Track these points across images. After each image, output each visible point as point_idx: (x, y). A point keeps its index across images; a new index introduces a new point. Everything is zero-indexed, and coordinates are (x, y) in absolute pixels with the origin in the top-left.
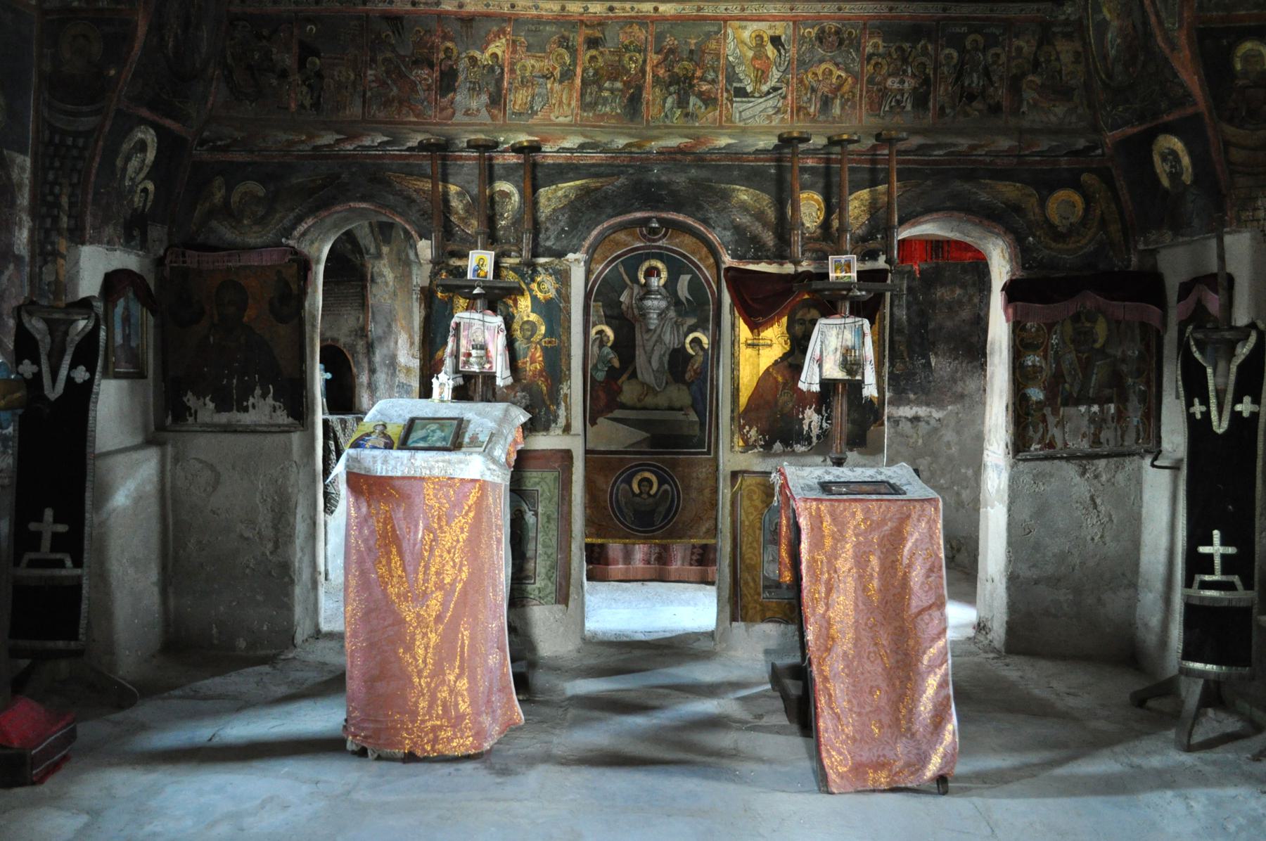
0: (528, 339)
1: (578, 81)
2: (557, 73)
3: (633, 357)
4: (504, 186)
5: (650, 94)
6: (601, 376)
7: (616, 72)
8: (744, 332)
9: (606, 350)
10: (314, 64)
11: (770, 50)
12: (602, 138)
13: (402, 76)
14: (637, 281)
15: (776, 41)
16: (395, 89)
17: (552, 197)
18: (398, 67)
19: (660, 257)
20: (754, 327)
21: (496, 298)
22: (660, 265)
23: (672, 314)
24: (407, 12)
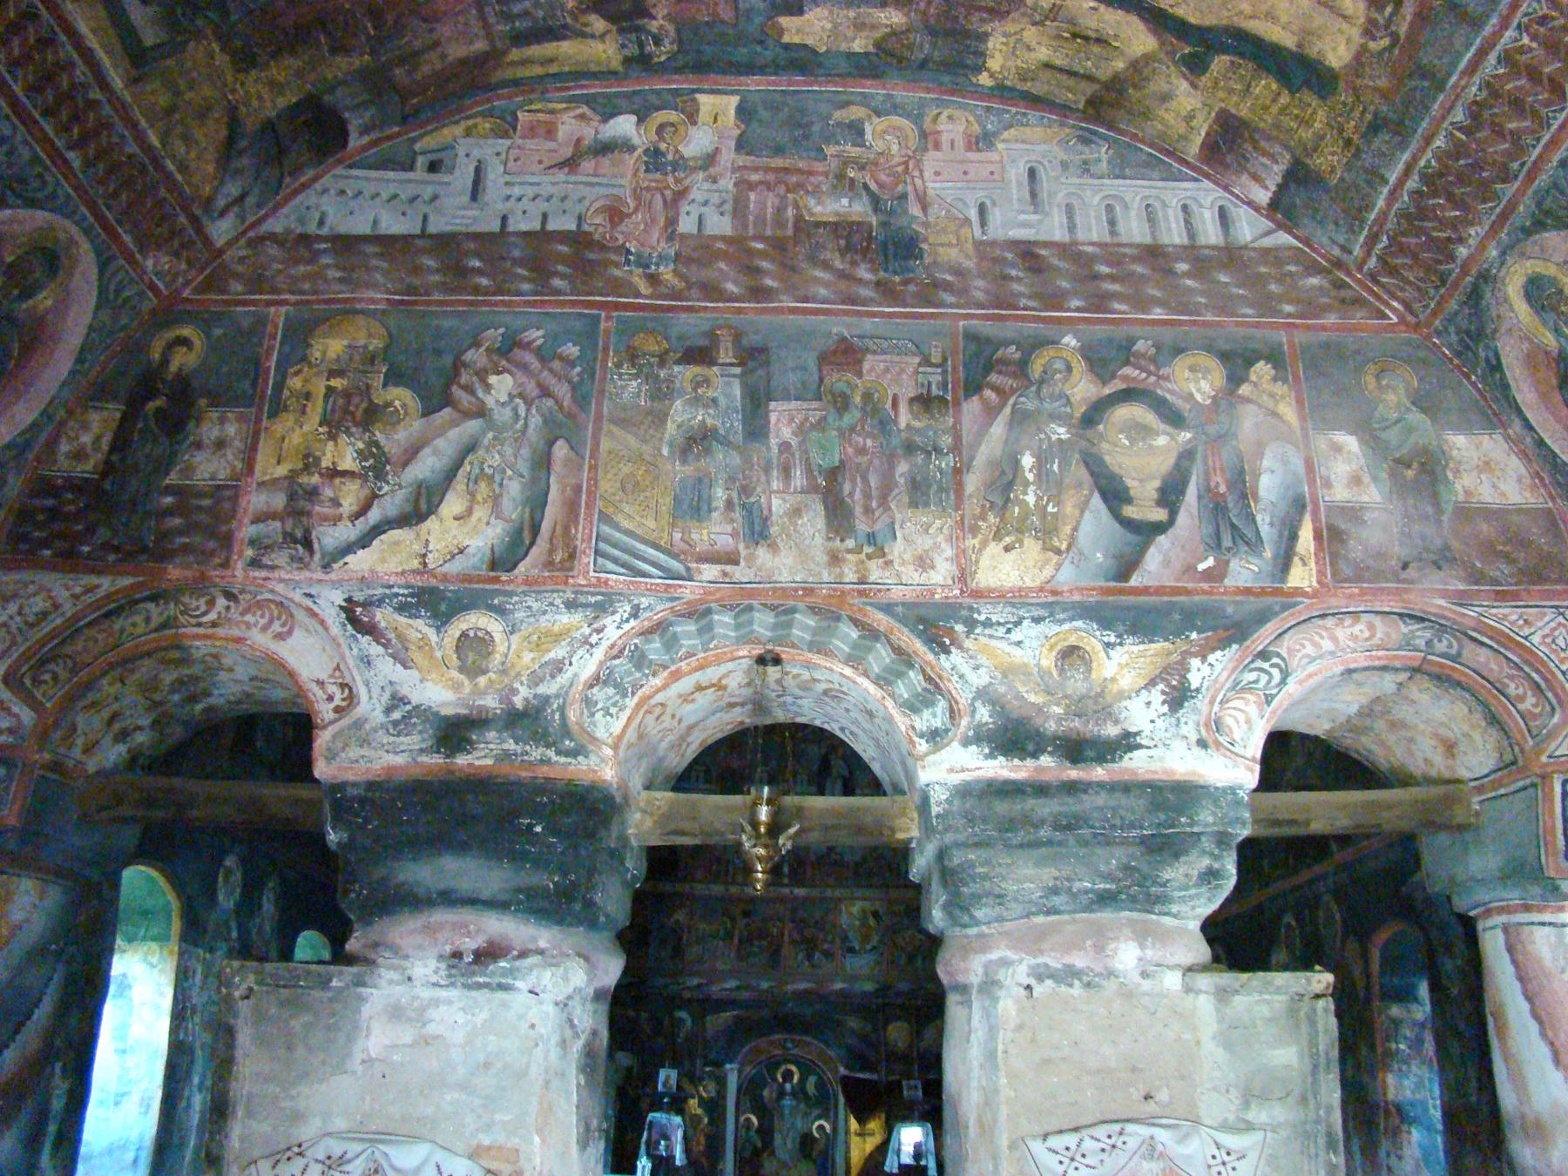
0: (695, 1129)
1: (736, 941)
2: (722, 933)
3: (772, 1138)
4: (683, 1014)
5: (786, 950)
6: (747, 1154)
7: (762, 934)
8: (854, 1124)
9: (752, 1133)
11: (872, 922)
12: (754, 983)
14: (775, 1079)
15: (875, 914)
17: (717, 1022)
19: (790, 1061)
20: (861, 1121)
21: (677, 1104)
22: (794, 1068)
23: (802, 1106)
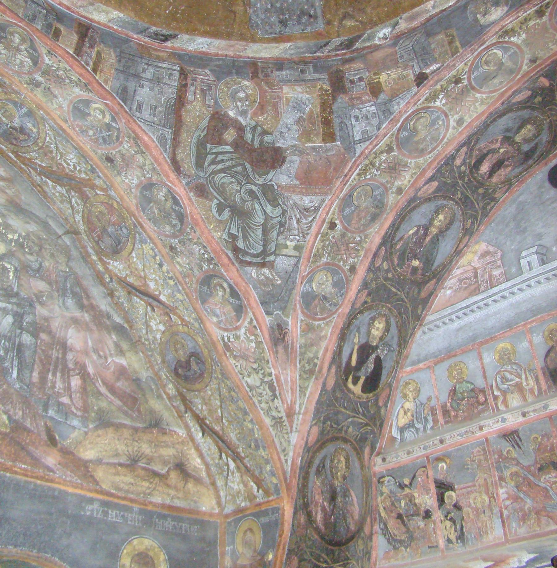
10: (450, 497)
13: (530, 485)
16: (528, 501)
18: (525, 478)
24: (521, 424)
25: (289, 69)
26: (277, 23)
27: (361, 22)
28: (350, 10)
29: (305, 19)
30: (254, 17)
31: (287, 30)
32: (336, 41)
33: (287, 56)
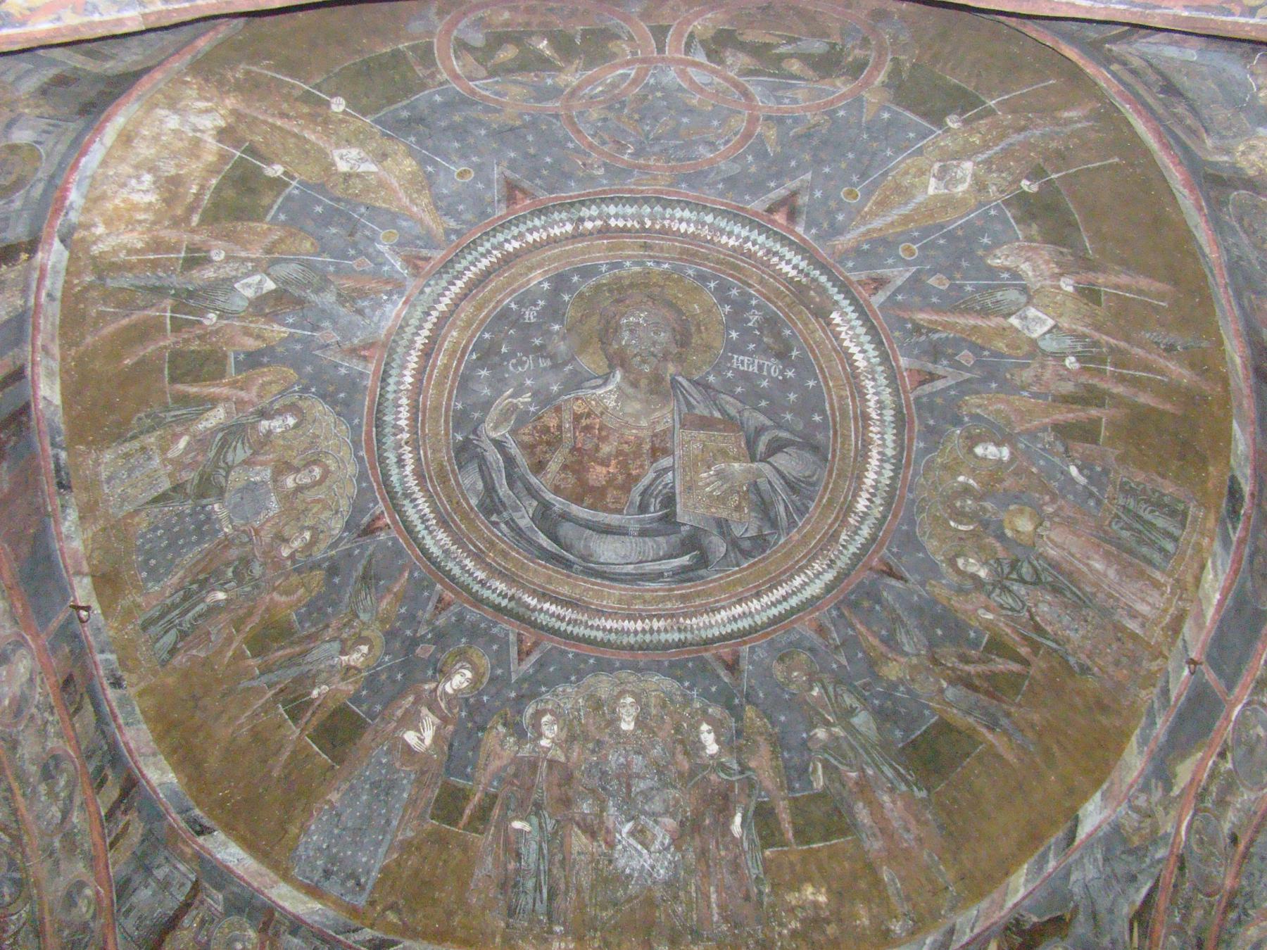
25: (305, 939)
26: (320, 870)
27: (404, 923)
28: (401, 902)
29: (351, 883)
30: (301, 849)
31: (327, 884)
32: (368, 933)
33: (309, 921)
